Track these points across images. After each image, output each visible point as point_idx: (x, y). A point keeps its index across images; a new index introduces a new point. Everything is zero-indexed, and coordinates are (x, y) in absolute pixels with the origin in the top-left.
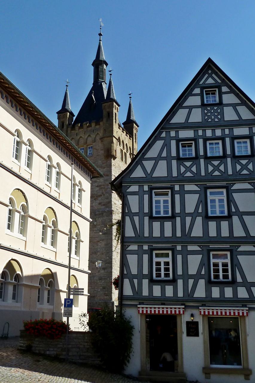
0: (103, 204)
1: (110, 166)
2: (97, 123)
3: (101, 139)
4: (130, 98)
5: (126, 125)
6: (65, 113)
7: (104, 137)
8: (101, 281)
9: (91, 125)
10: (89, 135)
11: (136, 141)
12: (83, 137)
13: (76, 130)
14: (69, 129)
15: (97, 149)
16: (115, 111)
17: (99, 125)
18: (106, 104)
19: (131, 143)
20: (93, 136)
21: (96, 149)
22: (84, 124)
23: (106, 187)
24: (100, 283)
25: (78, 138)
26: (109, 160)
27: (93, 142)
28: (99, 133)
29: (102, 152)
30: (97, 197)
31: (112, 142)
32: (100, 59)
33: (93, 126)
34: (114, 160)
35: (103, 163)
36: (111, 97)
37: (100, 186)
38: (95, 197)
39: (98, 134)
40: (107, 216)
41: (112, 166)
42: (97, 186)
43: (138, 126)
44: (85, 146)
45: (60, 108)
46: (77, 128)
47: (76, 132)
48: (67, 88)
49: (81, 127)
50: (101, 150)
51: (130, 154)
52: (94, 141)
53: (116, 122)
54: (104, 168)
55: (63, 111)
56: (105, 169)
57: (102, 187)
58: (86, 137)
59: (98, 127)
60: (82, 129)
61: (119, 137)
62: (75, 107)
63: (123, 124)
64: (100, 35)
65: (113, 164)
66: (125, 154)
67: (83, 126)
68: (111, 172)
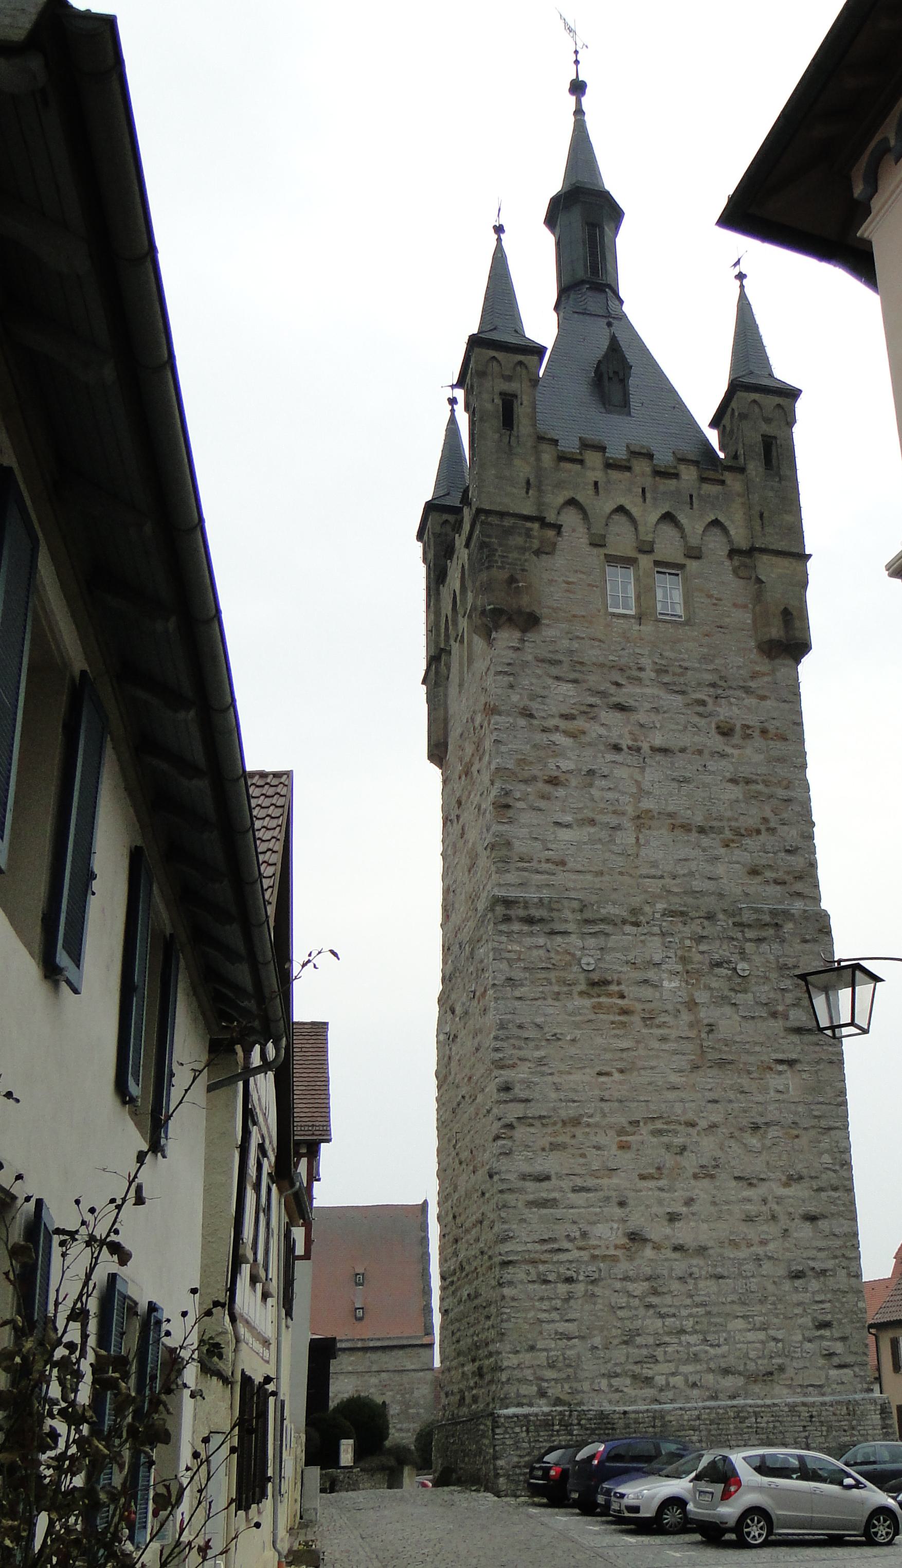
0: (769, 874)
8: (798, 1283)
21: (710, 596)
24: (796, 1298)
30: (737, 833)
37: (748, 782)
38: (728, 834)
40: (805, 941)
54: (763, 698)
56: (768, 702)
57: (760, 787)
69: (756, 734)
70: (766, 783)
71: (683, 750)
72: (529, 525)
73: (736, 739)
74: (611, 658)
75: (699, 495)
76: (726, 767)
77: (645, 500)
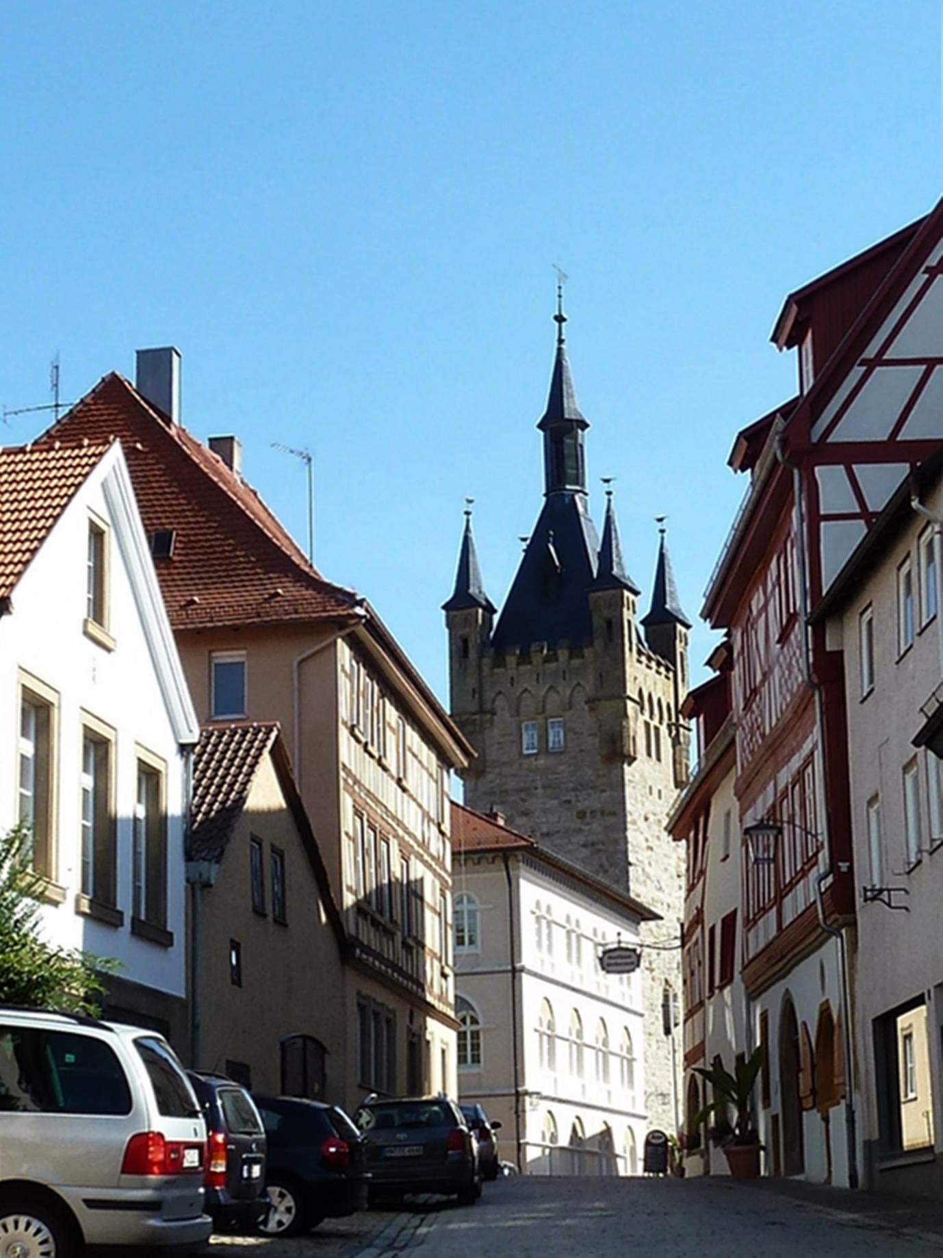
1: (620, 784)
2: (576, 651)
5: (654, 627)
6: (469, 611)
9: (555, 654)
10: (551, 687)
11: (683, 680)
14: (487, 661)
16: (627, 614)
17: (583, 657)
18: (599, 594)
23: (611, 849)
27: (564, 710)
28: (582, 682)
29: (596, 741)
31: (626, 716)
32: (566, 416)
33: (561, 659)
34: (629, 764)
35: (599, 776)
36: (615, 571)
37: (593, 844)
39: (579, 684)
42: (585, 846)
43: (688, 627)
44: (540, 717)
46: (511, 660)
47: (511, 673)
49: (525, 658)
50: (590, 735)
51: (669, 726)
53: (631, 649)
54: (603, 791)
55: (463, 603)
57: (600, 847)
58: (542, 693)
59: (576, 662)
61: (640, 691)
62: (496, 584)
63: (642, 622)
64: (560, 319)
65: (627, 777)
66: (657, 729)
68: (624, 803)
69: (599, 814)
70: (603, 844)
71: (558, 832)
73: (588, 819)
76: (581, 839)
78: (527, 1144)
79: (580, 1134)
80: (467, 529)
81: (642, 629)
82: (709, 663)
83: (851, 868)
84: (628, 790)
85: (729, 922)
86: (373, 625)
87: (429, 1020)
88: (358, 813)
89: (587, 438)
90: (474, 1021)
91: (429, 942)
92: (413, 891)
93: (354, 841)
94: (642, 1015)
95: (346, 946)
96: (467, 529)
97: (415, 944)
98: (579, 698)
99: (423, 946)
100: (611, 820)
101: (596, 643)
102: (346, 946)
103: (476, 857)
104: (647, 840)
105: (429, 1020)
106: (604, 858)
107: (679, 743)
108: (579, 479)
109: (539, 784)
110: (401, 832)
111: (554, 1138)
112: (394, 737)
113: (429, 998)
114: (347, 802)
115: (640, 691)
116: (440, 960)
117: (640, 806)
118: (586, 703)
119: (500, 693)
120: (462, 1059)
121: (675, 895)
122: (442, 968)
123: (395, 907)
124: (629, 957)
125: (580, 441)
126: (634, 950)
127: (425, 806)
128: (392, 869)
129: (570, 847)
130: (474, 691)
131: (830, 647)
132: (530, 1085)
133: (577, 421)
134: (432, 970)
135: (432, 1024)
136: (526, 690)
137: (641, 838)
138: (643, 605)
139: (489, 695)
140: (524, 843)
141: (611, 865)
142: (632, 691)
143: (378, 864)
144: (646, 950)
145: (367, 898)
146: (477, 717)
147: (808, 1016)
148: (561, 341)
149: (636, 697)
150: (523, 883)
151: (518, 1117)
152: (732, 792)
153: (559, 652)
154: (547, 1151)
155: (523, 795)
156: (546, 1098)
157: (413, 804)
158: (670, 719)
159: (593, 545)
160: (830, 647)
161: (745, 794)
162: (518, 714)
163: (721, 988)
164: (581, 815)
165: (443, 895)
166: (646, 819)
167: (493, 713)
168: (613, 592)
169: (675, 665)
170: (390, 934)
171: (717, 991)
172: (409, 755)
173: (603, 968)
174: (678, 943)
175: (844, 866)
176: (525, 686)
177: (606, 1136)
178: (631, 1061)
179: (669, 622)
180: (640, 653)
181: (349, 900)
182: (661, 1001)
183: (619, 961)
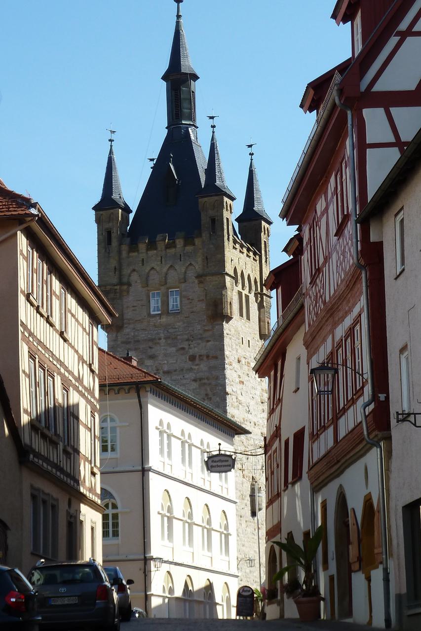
1: (220, 337)
3: (199, 276)
4: (251, 154)
5: (245, 224)
6: (112, 211)
7: (206, 275)
9: (174, 242)
10: (171, 266)
11: (266, 261)
12: (158, 268)
13: (140, 251)
14: (125, 248)
15: (190, 297)
16: (226, 214)
17: (194, 244)
18: (206, 199)
19: (258, 268)
20: (180, 268)
21: (189, 299)
22: (157, 240)
23: (214, 383)
25: (147, 271)
26: (217, 325)
28: (193, 263)
31: (224, 287)
33: (178, 246)
34: (227, 322)
35: (205, 331)
36: (218, 183)
37: (201, 379)
39: (191, 264)
41: (225, 339)
42: (195, 380)
43: (270, 223)
44: (163, 289)
45: (97, 198)
46: (142, 247)
47: (143, 255)
48: (111, 146)
49: (152, 245)
50: (199, 301)
52: (182, 281)
53: (228, 239)
54: (208, 341)
55: (107, 205)
56: (210, 343)
57: (206, 381)
58: (165, 270)
59: (189, 248)
60: (155, 251)
61: (235, 269)
62: (132, 191)
63: (236, 220)
66: (247, 297)
67: (155, 242)
69: (205, 358)
70: (208, 379)
71: (175, 371)
72: (116, 287)
73: (197, 362)
74: (149, 336)
75: (184, 253)
76: (191, 375)
77: (162, 263)
78: (152, 595)
79: (190, 588)
80: (111, 152)
81: (236, 225)
82: (286, 250)
83: (387, 398)
84: (227, 341)
85: (299, 436)
86: (43, 222)
87: (82, 505)
88: (32, 357)
89: (198, 87)
90: (115, 506)
91: (82, 450)
92: (71, 413)
93: (29, 376)
94: (235, 503)
95: (23, 453)
96: (111, 152)
97: (72, 451)
98: (191, 274)
99: (77, 451)
100: (213, 362)
101: (204, 235)
102: (23, 453)
103: (116, 388)
104: (239, 377)
105: (82, 505)
106: (208, 389)
107: (263, 307)
108: (191, 116)
109: (162, 335)
110: (62, 370)
111: (171, 591)
112: (58, 302)
113: (82, 490)
114: (24, 350)
115: (235, 269)
116: (91, 462)
117: (234, 352)
118: (196, 277)
119: (134, 270)
120: (105, 534)
121: (259, 416)
122: (92, 468)
123: (58, 424)
124: (228, 461)
125: (192, 89)
126: (230, 456)
127: (80, 352)
128: (56, 397)
129: (184, 382)
130: (115, 269)
131: (373, 238)
132: (154, 552)
133: (190, 74)
134: (84, 470)
135: (84, 509)
136: (153, 268)
137: (235, 375)
138: (238, 208)
139: (126, 271)
140: (151, 379)
141: (214, 394)
142: (229, 269)
143: (46, 394)
144: (239, 456)
145: (38, 417)
146: (118, 287)
147: (356, 504)
148: (179, 16)
149: (232, 274)
150: (151, 408)
151: (145, 576)
152: (302, 342)
153: (177, 241)
154: (166, 600)
155: (150, 344)
156: (166, 562)
157: (71, 351)
158: (256, 289)
159: (202, 163)
160: (373, 238)
161: (311, 345)
162: (147, 286)
163: (293, 484)
164: (192, 358)
165: (93, 416)
166: (239, 361)
167: (129, 284)
168: (216, 198)
169: (261, 253)
170: (54, 444)
171: (290, 486)
172: (69, 315)
173: (208, 469)
174: (262, 451)
175: (382, 397)
176: (153, 265)
177: (209, 588)
178: (227, 536)
179: (257, 220)
180: (235, 242)
181: (25, 419)
182: (249, 493)
183: (219, 464)
